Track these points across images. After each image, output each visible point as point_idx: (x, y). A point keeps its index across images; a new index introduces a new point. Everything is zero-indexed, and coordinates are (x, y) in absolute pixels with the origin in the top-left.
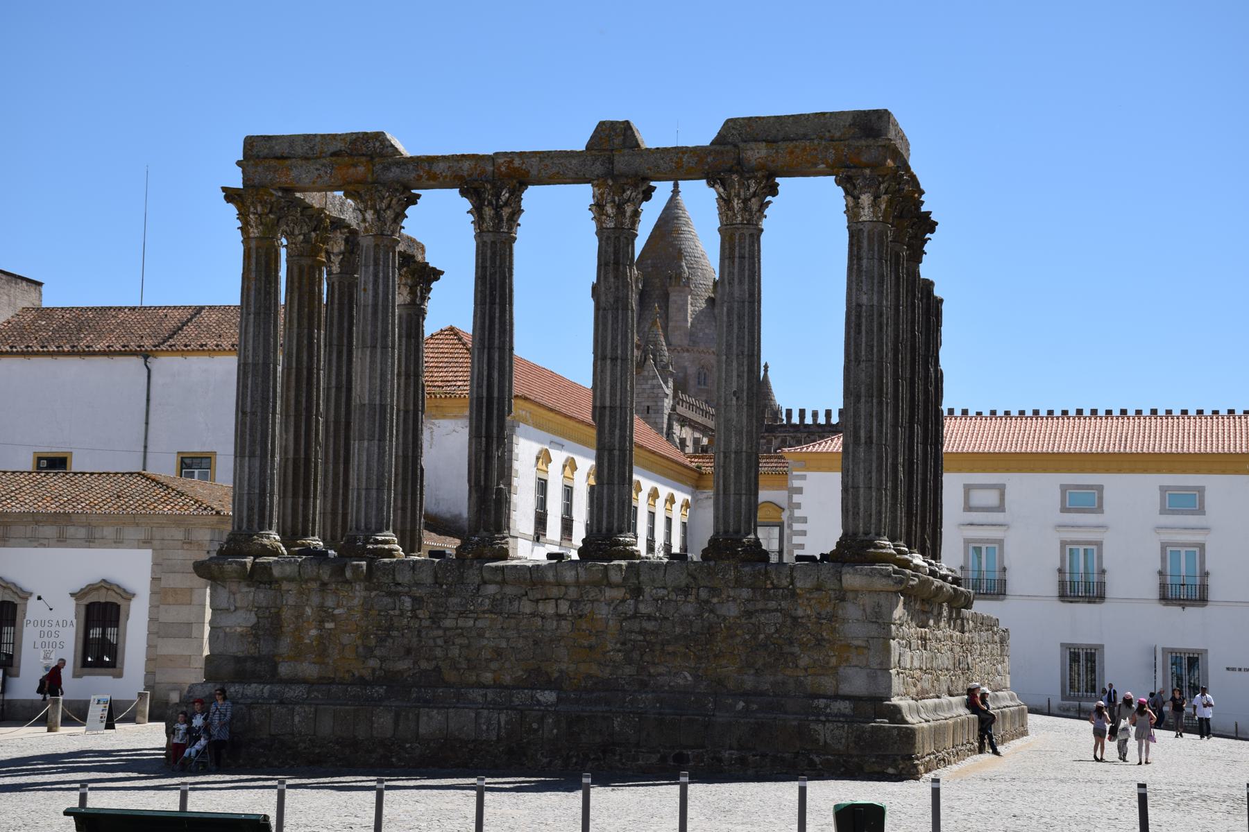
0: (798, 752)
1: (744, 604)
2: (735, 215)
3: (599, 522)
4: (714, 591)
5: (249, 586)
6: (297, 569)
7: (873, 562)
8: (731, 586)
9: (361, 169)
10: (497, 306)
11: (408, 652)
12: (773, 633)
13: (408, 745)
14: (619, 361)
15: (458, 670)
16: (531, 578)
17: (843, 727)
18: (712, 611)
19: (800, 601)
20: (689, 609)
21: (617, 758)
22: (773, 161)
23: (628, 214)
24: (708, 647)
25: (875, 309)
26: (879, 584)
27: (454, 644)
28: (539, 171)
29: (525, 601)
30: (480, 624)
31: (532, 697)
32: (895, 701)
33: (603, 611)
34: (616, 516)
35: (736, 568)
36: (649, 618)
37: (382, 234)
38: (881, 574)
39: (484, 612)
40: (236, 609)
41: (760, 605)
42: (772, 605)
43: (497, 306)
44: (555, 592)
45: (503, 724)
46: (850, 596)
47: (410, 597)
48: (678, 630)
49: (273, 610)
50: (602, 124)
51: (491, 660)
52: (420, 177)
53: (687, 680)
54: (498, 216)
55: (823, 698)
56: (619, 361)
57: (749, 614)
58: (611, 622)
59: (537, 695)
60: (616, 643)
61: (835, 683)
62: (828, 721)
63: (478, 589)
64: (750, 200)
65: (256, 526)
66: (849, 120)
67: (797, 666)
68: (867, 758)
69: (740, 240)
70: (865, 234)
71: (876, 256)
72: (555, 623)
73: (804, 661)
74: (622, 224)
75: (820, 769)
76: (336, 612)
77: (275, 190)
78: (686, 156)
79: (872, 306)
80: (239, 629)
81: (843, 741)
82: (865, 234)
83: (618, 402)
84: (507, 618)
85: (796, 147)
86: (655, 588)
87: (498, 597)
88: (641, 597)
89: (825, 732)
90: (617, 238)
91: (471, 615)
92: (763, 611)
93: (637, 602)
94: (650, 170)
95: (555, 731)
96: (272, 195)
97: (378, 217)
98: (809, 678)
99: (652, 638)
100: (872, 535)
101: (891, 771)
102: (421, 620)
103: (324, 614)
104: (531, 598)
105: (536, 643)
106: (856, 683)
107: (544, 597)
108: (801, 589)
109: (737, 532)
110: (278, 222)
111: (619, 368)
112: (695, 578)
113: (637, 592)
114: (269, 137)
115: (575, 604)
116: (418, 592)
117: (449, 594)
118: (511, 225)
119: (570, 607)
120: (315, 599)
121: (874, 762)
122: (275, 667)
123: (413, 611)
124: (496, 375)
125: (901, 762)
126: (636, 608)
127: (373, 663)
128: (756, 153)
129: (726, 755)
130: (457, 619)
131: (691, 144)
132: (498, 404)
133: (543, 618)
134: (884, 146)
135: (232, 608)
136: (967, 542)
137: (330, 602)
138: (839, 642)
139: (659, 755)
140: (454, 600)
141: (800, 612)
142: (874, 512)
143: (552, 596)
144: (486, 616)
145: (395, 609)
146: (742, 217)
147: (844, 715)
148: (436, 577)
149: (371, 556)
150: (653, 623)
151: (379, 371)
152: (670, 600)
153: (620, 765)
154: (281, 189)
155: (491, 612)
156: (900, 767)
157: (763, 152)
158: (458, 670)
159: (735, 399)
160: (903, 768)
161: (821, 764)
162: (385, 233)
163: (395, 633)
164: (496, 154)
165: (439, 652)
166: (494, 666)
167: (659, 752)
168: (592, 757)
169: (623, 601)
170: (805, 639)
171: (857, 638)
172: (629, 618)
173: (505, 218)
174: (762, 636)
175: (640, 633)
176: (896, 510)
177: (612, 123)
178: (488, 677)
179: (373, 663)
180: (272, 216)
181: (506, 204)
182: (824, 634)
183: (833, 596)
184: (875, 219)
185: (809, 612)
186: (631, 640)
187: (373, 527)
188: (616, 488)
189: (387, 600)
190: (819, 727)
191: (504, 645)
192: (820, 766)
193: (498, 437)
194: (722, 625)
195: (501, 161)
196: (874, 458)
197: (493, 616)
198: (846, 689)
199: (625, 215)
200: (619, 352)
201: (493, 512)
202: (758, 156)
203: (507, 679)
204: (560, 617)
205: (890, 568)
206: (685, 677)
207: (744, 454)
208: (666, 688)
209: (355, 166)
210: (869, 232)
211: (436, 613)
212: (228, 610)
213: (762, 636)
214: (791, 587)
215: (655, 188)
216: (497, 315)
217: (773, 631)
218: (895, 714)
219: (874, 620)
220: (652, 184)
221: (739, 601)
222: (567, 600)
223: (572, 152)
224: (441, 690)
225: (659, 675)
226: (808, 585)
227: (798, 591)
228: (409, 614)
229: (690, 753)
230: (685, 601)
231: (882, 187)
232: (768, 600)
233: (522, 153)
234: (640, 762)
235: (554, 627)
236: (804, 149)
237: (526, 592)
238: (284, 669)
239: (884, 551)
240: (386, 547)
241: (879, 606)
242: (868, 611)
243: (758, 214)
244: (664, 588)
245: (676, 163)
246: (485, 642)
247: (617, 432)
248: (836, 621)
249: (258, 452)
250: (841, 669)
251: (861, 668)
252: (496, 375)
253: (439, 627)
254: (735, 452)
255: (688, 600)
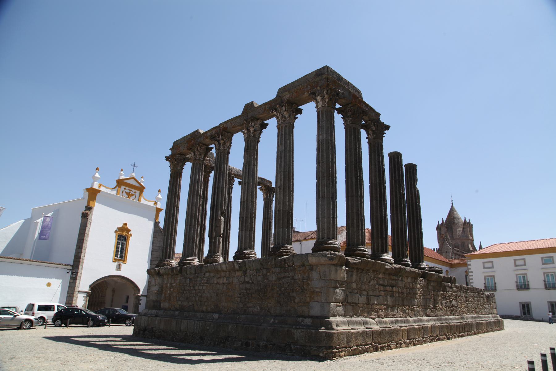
0: (287, 344)
1: (277, 274)
2: (279, 120)
3: (241, 246)
4: (268, 270)
5: (158, 277)
6: (164, 270)
7: (323, 251)
8: (274, 267)
9: (193, 142)
10: (218, 174)
11: (187, 299)
12: (287, 287)
13: (178, 333)
14: (247, 184)
15: (198, 305)
16: (215, 269)
17: (304, 332)
18: (267, 279)
19: (297, 272)
20: (260, 278)
21: (229, 343)
22: (291, 97)
23: (252, 131)
24: (265, 294)
25: (325, 140)
26: (323, 260)
27: (197, 296)
28: (230, 126)
29: (215, 279)
30: (204, 288)
31: (212, 316)
32: (332, 319)
33: (235, 281)
34: (243, 243)
35: (275, 259)
36: (248, 283)
37: (195, 159)
38: (322, 255)
39: (205, 284)
40: (156, 285)
41: (283, 275)
42: (287, 274)
43: (218, 174)
44: (223, 274)
45: (200, 326)
46: (314, 267)
47: (189, 279)
48: (256, 288)
49: (162, 285)
50: (246, 105)
51: (205, 302)
52: (204, 139)
53: (258, 310)
54: (220, 144)
55: (301, 317)
56: (247, 184)
57: (279, 279)
58: (237, 285)
59: (214, 315)
60: (238, 294)
61: (308, 309)
62: (299, 328)
63: (204, 275)
64: (284, 113)
65: (164, 258)
66: (315, 74)
67: (295, 302)
68: (312, 348)
69: (281, 128)
70: (320, 112)
71: (325, 120)
72: (222, 286)
73: (296, 301)
74: (250, 135)
75: (294, 353)
76: (174, 285)
77: (177, 155)
78: (267, 106)
79: (324, 140)
80: (155, 291)
81: (304, 338)
82: (320, 112)
83: (246, 199)
84: (211, 285)
85: (297, 89)
86: (251, 270)
87: (209, 277)
88: (246, 275)
89: (298, 334)
90: (248, 141)
91: (202, 285)
92: (284, 277)
93: (245, 276)
94: (257, 114)
95: (213, 330)
96: (176, 156)
97: (194, 154)
98: (299, 307)
99: (248, 291)
100: (325, 238)
101: (321, 355)
102: (191, 287)
103: (172, 286)
104: (217, 277)
105: (217, 295)
106: (316, 310)
107: (220, 277)
108: (297, 266)
109: (279, 244)
110: (178, 164)
111: (246, 186)
112: (262, 265)
113: (245, 272)
114: (177, 140)
115: (228, 278)
116: (191, 276)
117: (198, 277)
118: (224, 146)
119: (226, 280)
120: (170, 281)
121: (315, 350)
122: (160, 304)
123: (189, 283)
124: (216, 197)
125: (324, 350)
126: (244, 279)
127: (179, 303)
128: (287, 96)
129: (261, 344)
130: (199, 286)
131: (267, 101)
132: (216, 207)
133: (219, 284)
134: (326, 78)
135: (155, 284)
136: (517, 275)
137: (173, 282)
138: (310, 290)
139: (241, 342)
140: (199, 279)
141: (296, 277)
142: (326, 228)
143: (222, 276)
144: (205, 284)
145: (185, 283)
146: (282, 120)
147: (308, 326)
148: (195, 271)
149: (183, 265)
150: (249, 285)
151: (191, 203)
152: (254, 275)
153: (229, 346)
154: (179, 154)
155: (207, 283)
156: (325, 353)
157: (288, 95)
158: (198, 305)
159: (279, 189)
160: (326, 354)
161: (294, 350)
162: (196, 159)
163: (185, 292)
164: (219, 125)
165: (194, 299)
166: (206, 304)
167: (241, 341)
168: (222, 342)
169: (241, 276)
170: (298, 289)
171: (317, 288)
172: (242, 283)
173: (222, 144)
174: (283, 289)
175: (245, 289)
176: (359, 232)
177: (248, 104)
178: (204, 308)
179: (179, 303)
180: (176, 162)
181: (222, 139)
182: (305, 286)
183: (308, 268)
184: (324, 106)
185: (299, 277)
186: (242, 293)
187: (186, 255)
188: (244, 232)
189: (184, 280)
190: (294, 331)
191: (209, 296)
192: (294, 351)
193: (216, 219)
194: (270, 285)
195: (221, 127)
196: (325, 203)
197: (207, 285)
198: (313, 312)
199: (250, 132)
200: (247, 180)
201: (213, 246)
202: (287, 97)
203: (209, 309)
204: (224, 284)
205: (328, 253)
206: (257, 308)
207: (282, 211)
208: (251, 313)
209: (191, 141)
210: (322, 111)
211: (195, 284)
212: (154, 285)
213: (283, 289)
214: (293, 266)
215: (267, 124)
216: (218, 176)
217: (287, 286)
218: (329, 326)
219: (323, 278)
220: (266, 122)
221: (276, 274)
222: (226, 277)
223: (237, 116)
224: (191, 313)
225: (250, 307)
226: (299, 264)
227: (296, 267)
228: (188, 285)
229: (251, 342)
230: (259, 275)
231: (324, 92)
232: (286, 273)
233: (225, 122)
234: (235, 345)
235: (222, 288)
236: (300, 89)
237: (216, 275)
238: (162, 305)
239: (332, 245)
240: (188, 262)
241: (325, 271)
242: (321, 274)
243: (288, 118)
244: (253, 270)
245: (264, 109)
246: (204, 295)
247: (245, 210)
248: (309, 280)
249: (166, 234)
250: (311, 303)
251: (318, 302)
252: (216, 197)
253: (195, 290)
254: (278, 211)
255: (260, 274)
